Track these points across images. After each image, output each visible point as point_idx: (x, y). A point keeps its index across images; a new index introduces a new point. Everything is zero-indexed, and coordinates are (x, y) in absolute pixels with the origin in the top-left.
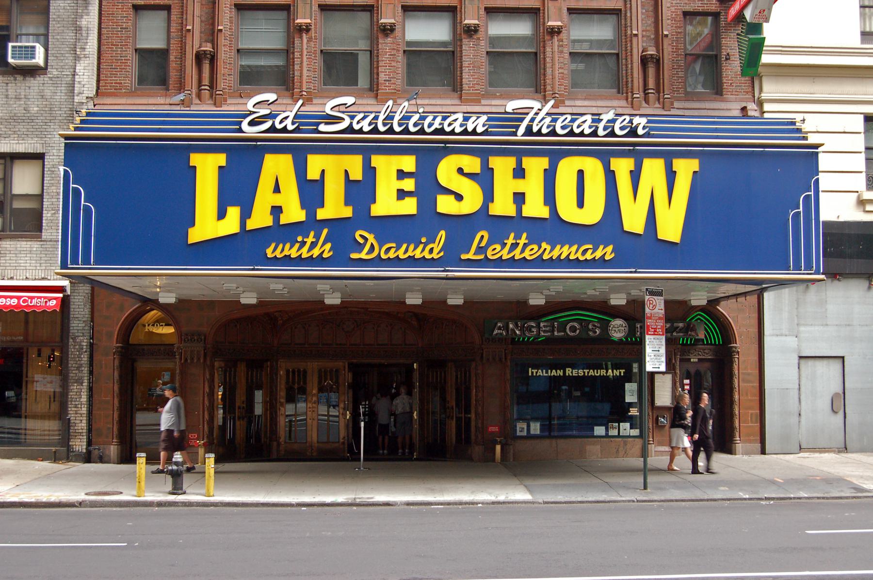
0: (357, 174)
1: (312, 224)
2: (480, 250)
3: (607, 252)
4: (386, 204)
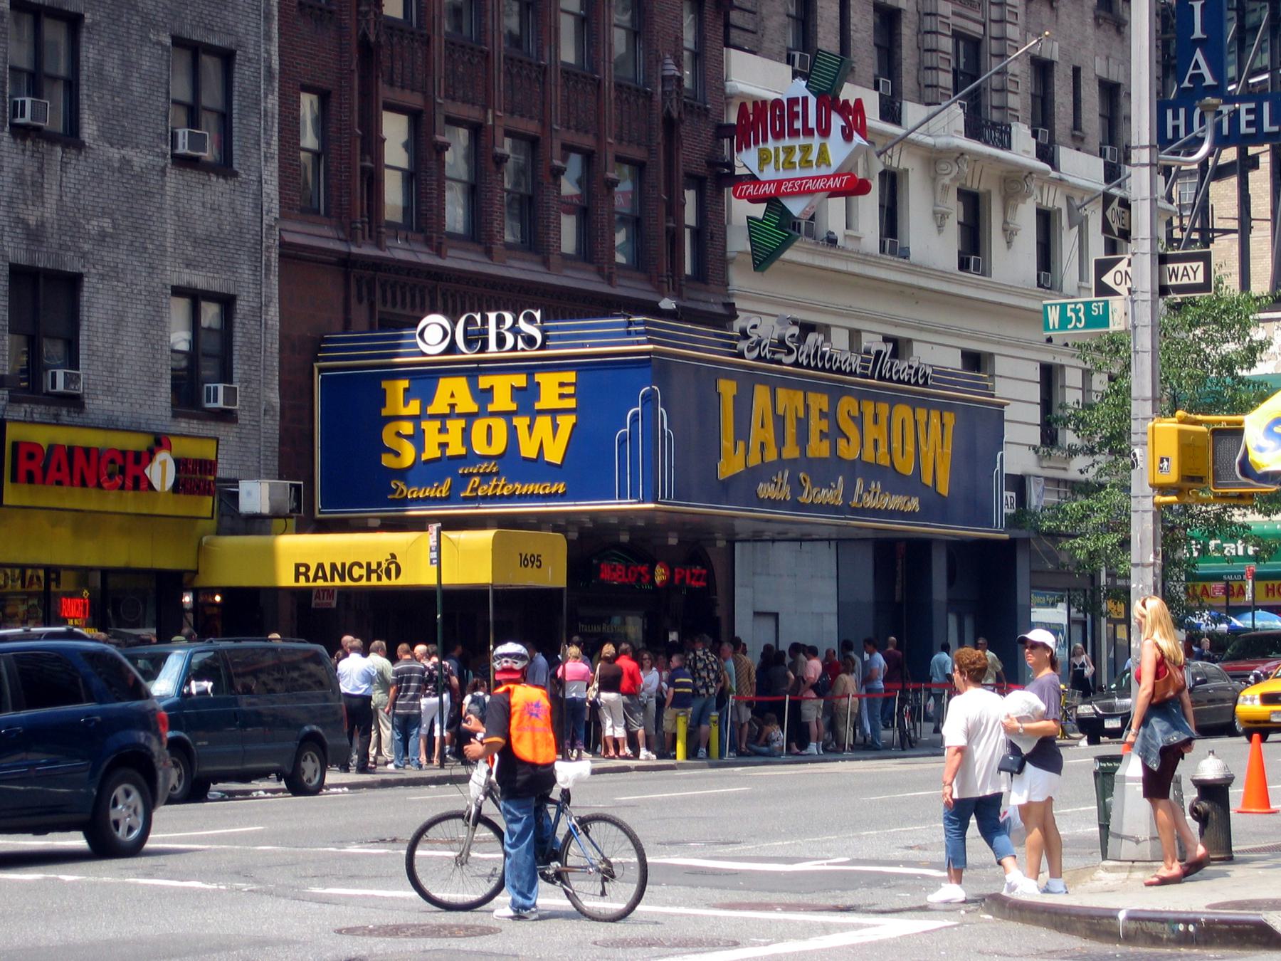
0: (801, 414)
1: (781, 463)
2: (860, 497)
3: (914, 504)
4: (818, 449)
